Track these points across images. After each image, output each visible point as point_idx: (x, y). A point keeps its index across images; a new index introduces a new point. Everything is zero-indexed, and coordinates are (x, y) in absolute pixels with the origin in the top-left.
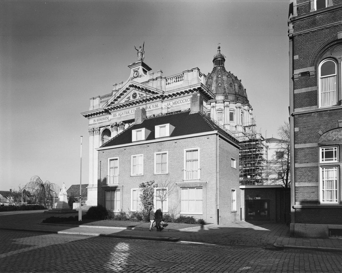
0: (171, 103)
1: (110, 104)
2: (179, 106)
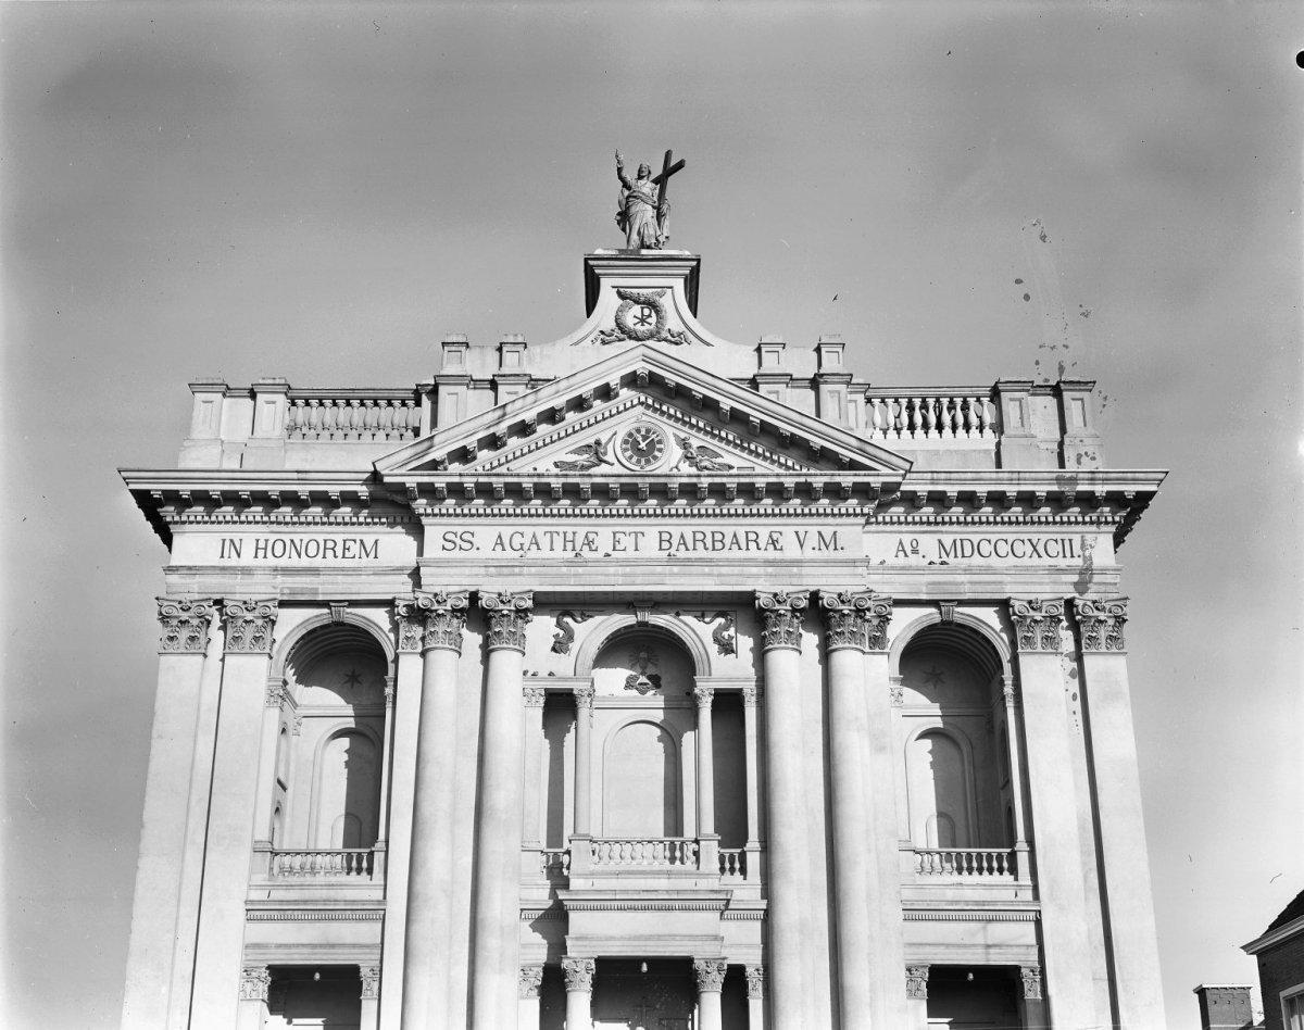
0: (929, 543)
1: (442, 462)
2: (989, 570)
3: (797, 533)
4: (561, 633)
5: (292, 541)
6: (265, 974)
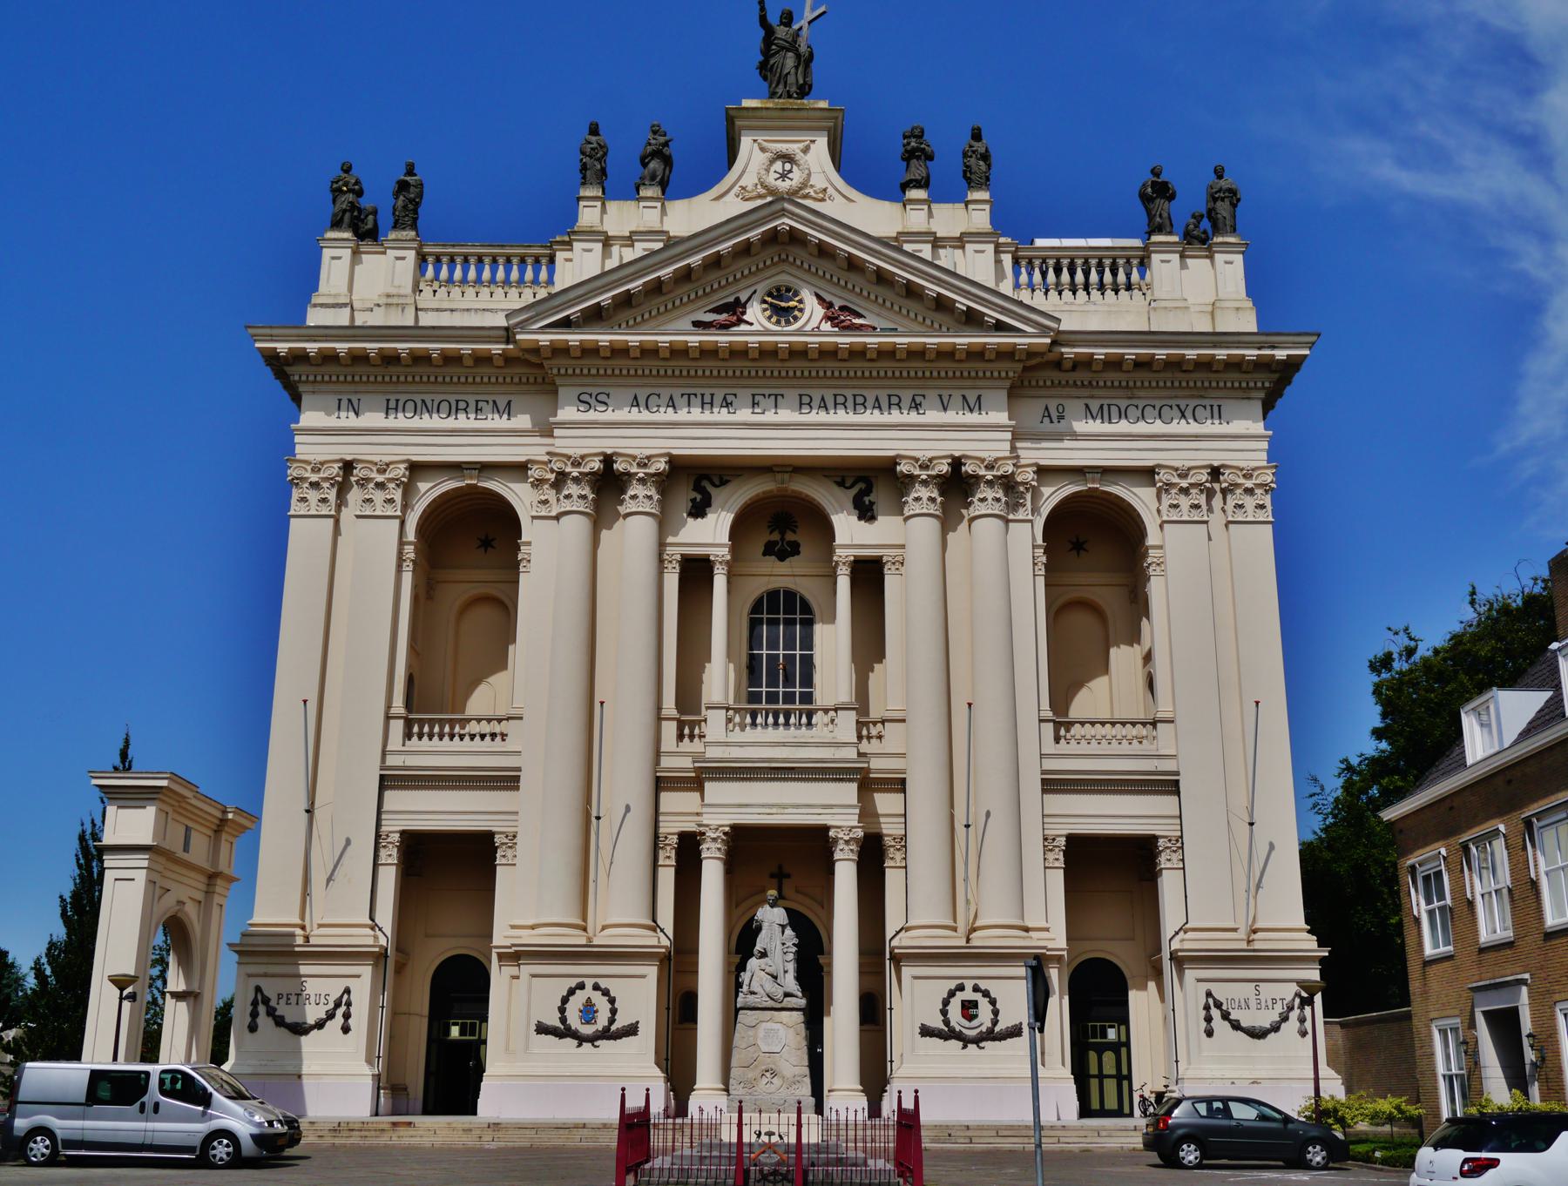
3: (940, 396)
4: (699, 497)
5: (423, 401)
6: (396, 837)
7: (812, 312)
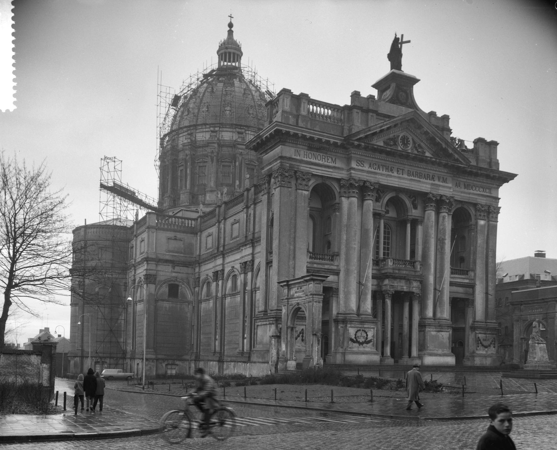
4: (378, 195)
7: (410, 146)
